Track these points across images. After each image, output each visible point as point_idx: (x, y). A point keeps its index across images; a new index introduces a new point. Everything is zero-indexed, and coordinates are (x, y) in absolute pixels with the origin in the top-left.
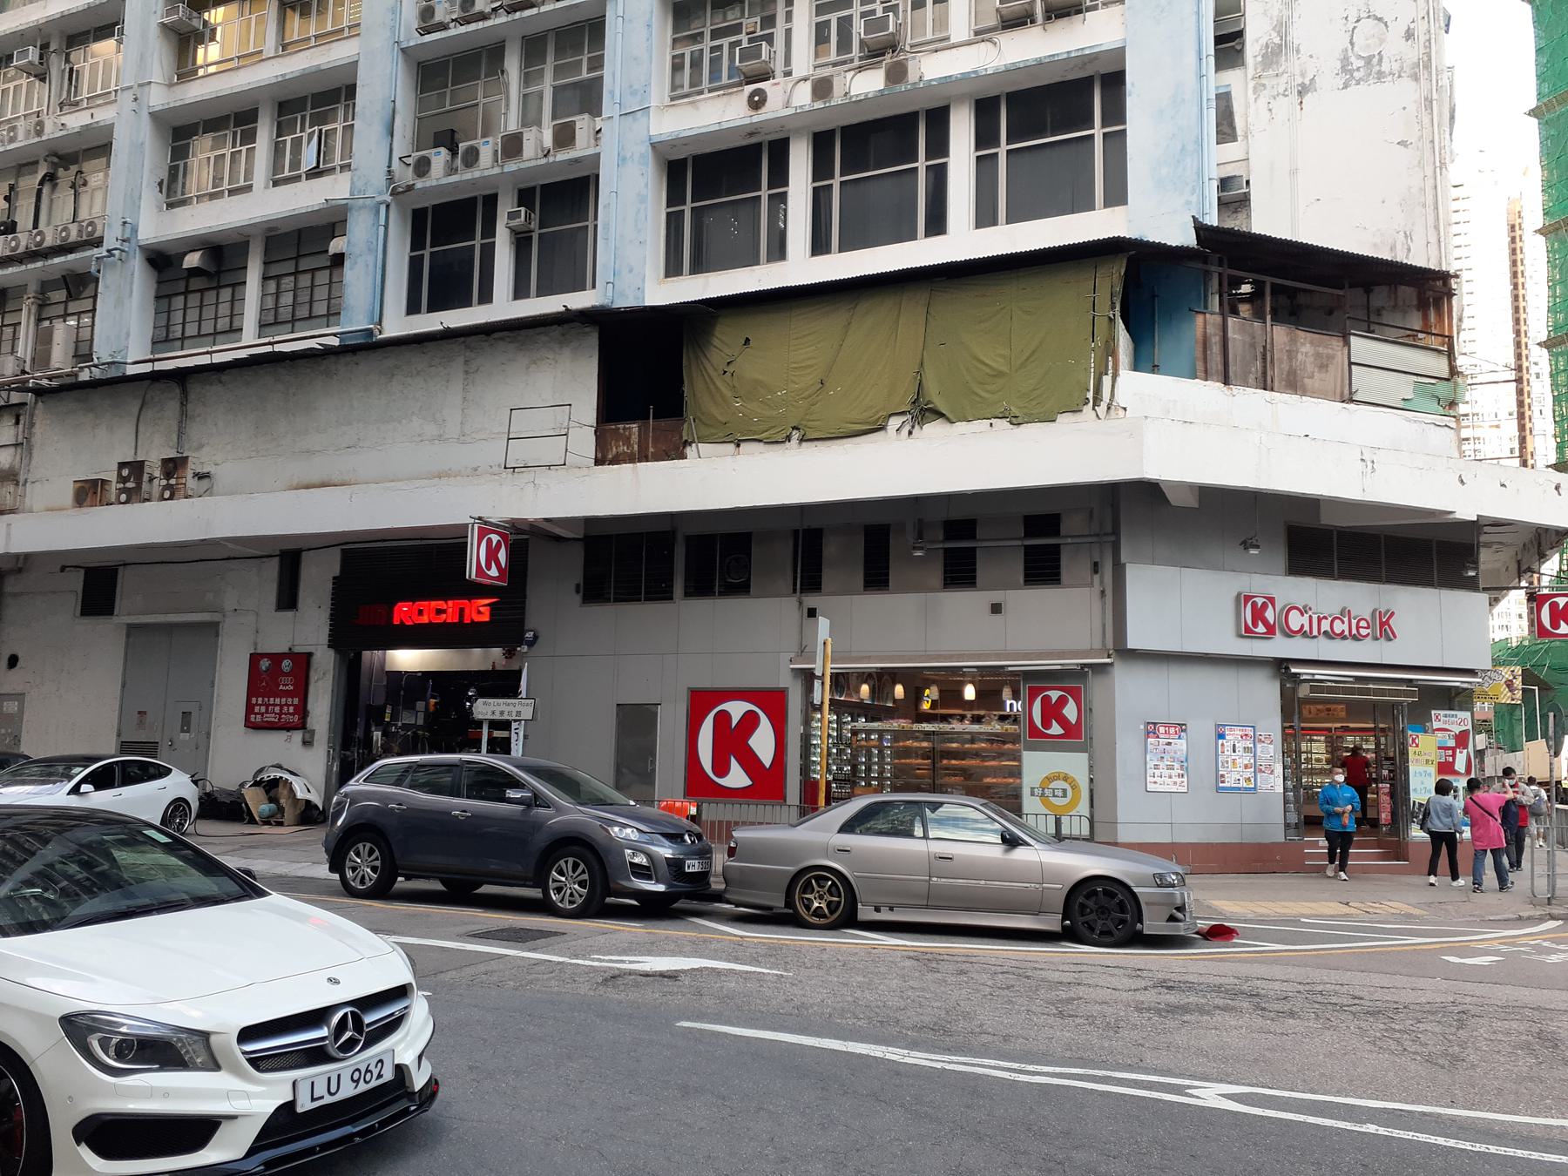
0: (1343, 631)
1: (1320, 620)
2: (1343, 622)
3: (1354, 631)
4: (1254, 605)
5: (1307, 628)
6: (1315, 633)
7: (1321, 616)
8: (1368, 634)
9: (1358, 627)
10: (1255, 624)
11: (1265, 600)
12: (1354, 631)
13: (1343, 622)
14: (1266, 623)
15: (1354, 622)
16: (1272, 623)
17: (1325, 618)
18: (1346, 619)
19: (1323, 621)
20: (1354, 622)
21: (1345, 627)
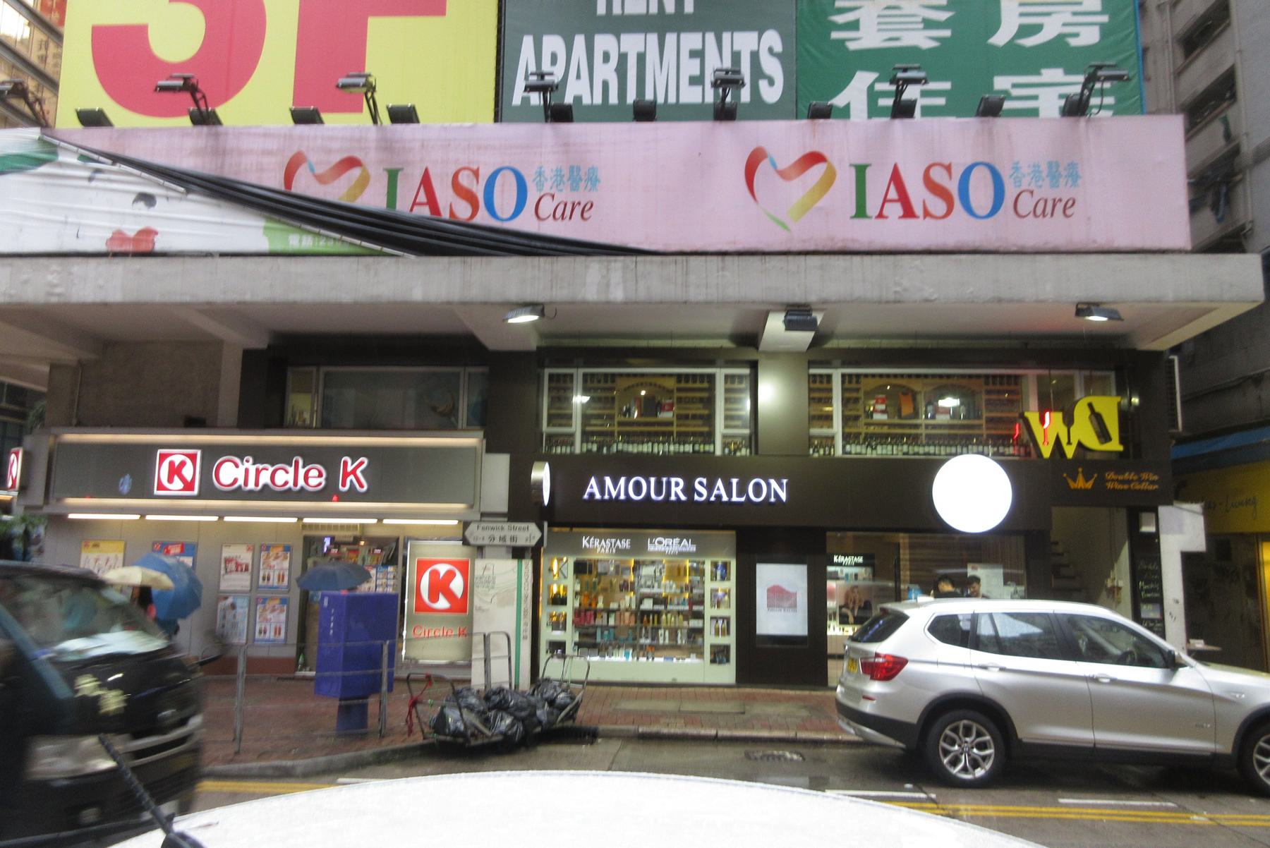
0: (286, 483)
1: (258, 472)
2: (287, 472)
3: (301, 482)
4: (172, 464)
5: (241, 482)
6: (251, 485)
7: (260, 469)
8: (320, 484)
9: (306, 478)
10: (170, 480)
11: (183, 458)
12: (301, 482)
13: (287, 472)
14: (183, 479)
15: (302, 472)
16: (189, 478)
17: (267, 469)
18: (291, 470)
19: (264, 472)
20: (302, 472)
21: (290, 477)
